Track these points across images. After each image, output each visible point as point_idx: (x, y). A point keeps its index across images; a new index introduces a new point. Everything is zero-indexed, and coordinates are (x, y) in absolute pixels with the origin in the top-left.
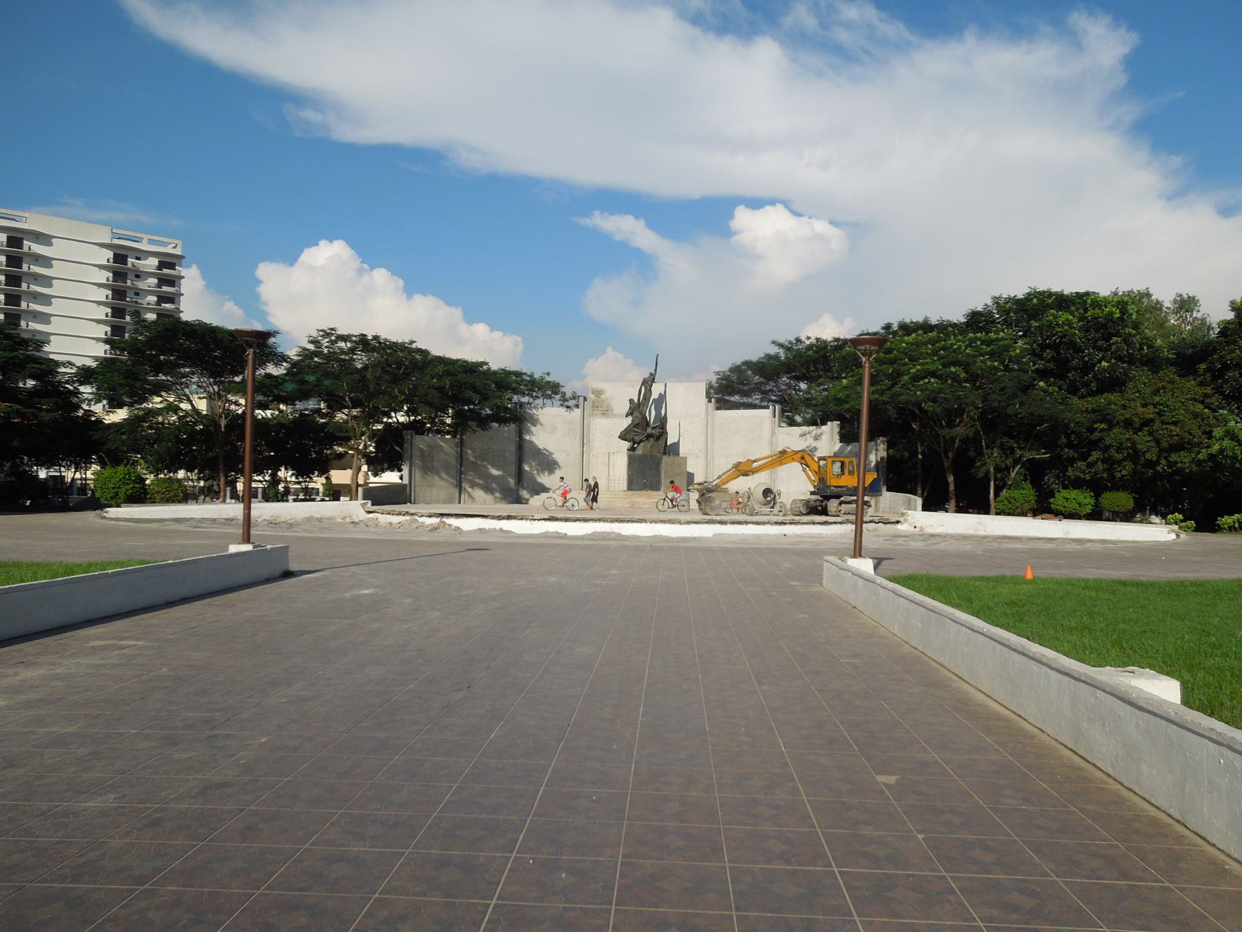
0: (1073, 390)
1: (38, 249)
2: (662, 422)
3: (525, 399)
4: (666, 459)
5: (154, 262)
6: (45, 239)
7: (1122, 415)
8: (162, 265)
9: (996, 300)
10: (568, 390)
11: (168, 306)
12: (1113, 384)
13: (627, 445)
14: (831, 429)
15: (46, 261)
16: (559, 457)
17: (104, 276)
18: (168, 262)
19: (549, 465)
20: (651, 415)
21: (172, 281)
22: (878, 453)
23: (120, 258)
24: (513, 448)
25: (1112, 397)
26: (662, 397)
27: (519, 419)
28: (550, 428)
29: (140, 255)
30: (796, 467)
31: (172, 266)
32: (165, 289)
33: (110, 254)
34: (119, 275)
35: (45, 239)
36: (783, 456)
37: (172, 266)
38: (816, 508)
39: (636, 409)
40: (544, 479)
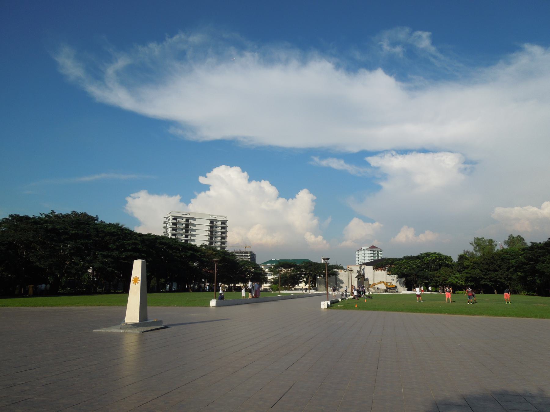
0: (431, 271)
1: (193, 222)
2: (364, 274)
3: (336, 270)
4: (365, 282)
5: (220, 223)
6: (194, 219)
7: (436, 275)
8: (222, 223)
9: (421, 254)
10: (345, 268)
11: (224, 235)
12: (435, 270)
13: (357, 279)
14: (396, 276)
15: (194, 225)
16: (344, 281)
17: (208, 228)
18: (224, 222)
19: (342, 283)
20: (362, 273)
21: (224, 228)
22: (403, 280)
23: (212, 223)
24: (334, 280)
25: (435, 272)
26: (363, 270)
27: (336, 274)
28: (342, 275)
29: (217, 221)
30: (383, 284)
31: (224, 223)
32: (223, 230)
33: (209, 221)
34: (212, 227)
35: (194, 219)
36: (380, 282)
37: (224, 223)
38: (386, 291)
39: (359, 272)
40: (341, 285)
